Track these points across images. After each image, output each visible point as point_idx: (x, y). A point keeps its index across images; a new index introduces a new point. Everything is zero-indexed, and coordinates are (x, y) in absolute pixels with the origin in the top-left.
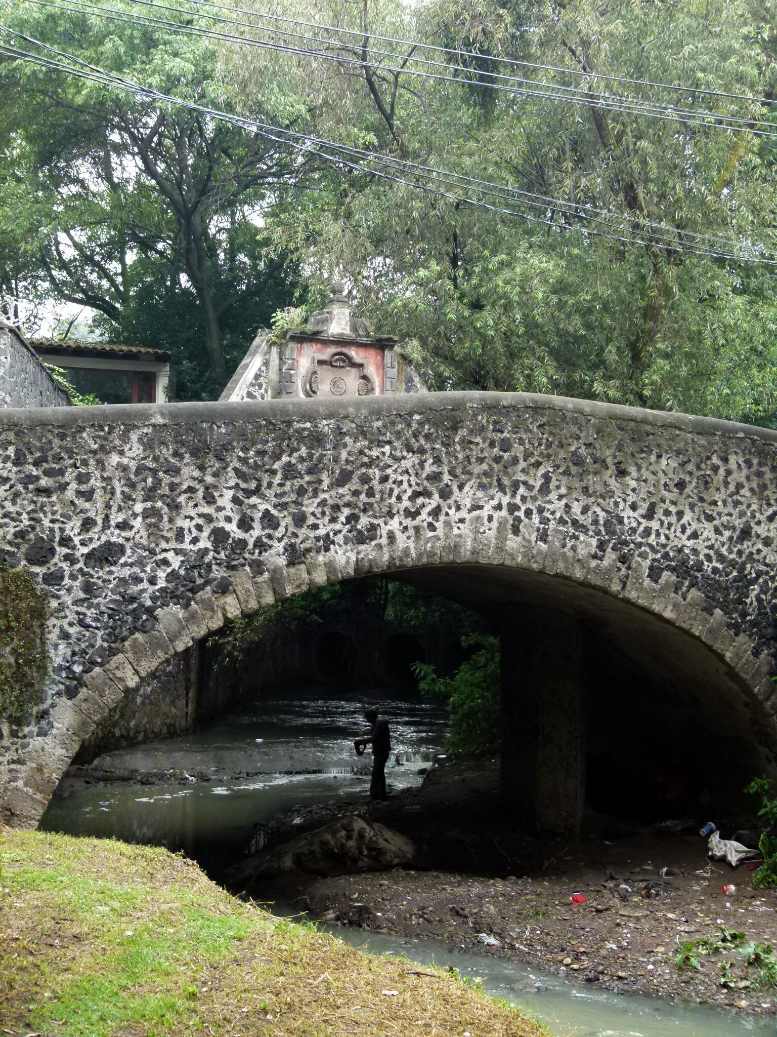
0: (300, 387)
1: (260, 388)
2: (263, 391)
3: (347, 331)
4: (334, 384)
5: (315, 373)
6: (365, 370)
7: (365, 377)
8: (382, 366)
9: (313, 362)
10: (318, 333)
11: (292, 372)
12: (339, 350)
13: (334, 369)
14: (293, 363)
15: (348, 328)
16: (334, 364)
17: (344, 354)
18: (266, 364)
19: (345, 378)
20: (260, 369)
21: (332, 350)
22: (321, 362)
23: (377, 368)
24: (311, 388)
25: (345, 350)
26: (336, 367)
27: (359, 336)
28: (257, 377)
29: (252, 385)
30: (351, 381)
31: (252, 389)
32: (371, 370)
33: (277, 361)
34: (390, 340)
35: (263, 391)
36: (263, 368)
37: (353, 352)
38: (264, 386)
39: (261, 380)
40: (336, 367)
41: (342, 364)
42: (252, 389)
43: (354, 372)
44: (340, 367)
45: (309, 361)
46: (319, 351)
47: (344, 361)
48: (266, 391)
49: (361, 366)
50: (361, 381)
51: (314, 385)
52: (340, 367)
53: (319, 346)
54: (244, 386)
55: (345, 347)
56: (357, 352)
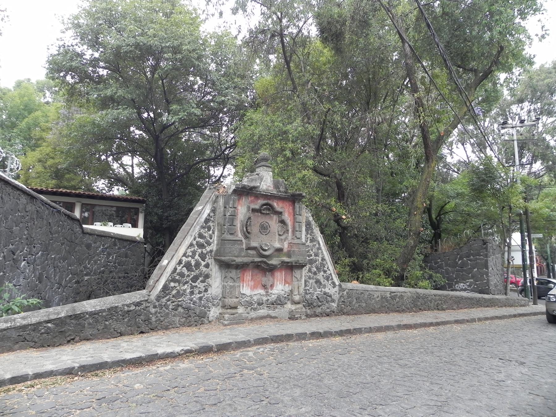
0: (239, 229)
1: (209, 230)
2: (211, 232)
3: (271, 188)
5: (249, 218)
7: (283, 222)
9: (249, 210)
10: (255, 187)
12: (265, 202)
13: (263, 216)
14: (234, 211)
15: (272, 186)
16: (263, 212)
18: (214, 211)
20: (209, 215)
21: (261, 202)
22: (254, 210)
24: (247, 230)
25: (270, 202)
26: (264, 214)
27: (280, 191)
28: (207, 221)
29: (202, 227)
30: (273, 223)
31: (202, 231)
32: (287, 217)
33: (222, 209)
34: (300, 195)
35: (211, 232)
36: (212, 214)
37: (276, 205)
38: (212, 228)
39: (211, 224)
40: (264, 214)
41: (268, 212)
42: (202, 231)
43: (275, 217)
44: (267, 214)
45: (246, 209)
46: (252, 202)
47: (269, 210)
48: (213, 233)
49: (281, 213)
50: (280, 224)
51: (249, 228)
52: (267, 214)
53: (253, 198)
55: (270, 199)
56: (277, 203)
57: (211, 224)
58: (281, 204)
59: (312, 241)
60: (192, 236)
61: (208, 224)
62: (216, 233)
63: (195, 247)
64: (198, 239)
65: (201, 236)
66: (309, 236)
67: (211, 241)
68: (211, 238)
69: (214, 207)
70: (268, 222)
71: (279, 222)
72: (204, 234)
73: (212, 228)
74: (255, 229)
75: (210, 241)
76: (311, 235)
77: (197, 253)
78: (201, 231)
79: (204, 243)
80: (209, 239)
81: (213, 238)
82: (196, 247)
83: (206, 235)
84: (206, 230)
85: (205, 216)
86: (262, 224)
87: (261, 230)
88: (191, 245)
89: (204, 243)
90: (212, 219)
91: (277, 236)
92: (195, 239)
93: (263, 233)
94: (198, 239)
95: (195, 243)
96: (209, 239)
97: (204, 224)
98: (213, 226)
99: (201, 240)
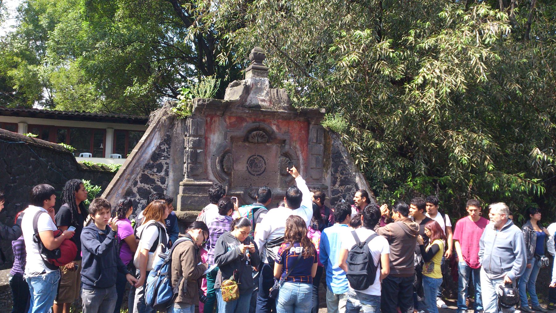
1: (159, 171)
4: (252, 163)
6: (287, 147)
8: (305, 141)
11: (199, 151)
17: (264, 130)
19: (265, 156)
20: (159, 147)
23: (302, 144)
28: (156, 156)
29: (148, 166)
35: (163, 174)
38: (165, 168)
39: (162, 161)
43: (275, 148)
47: (263, 137)
48: (167, 174)
54: (138, 169)
57: (162, 161)
58: (284, 129)
59: (343, 183)
60: (128, 180)
61: (158, 162)
62: (171, 174)
63: (136, 196)
64: (139, 185)
65: (145, 179)
66: (338, 175)
67: (163, 186)
68: (163, 183)
69: (168, 136)
70: (263, 155)
71: (282, 155)
72: (151, 177)
73: (165, 168)
74: (241, 167)
75: (161, 187)
76: (342, 174)
77: (139, 205)
78: (146, 173)
79: (152, 190)
80: (159, 183)
81: (166, 183)
82: (138, 197)
83: (155, 178)
84: (155, 170)
85: (152, 148)
86: (251, 158)
87: (249, 169)
88: (129, 193)
89: (152, 190)
90: (165, 154)
91: (279, 177)
92: (135, 183)
93: (253, 173)
94: (139, 185)
95: (135, 190)
96: (159, 183)
97: (151, 162)
98: (166, 163)
99: (146, 186)
